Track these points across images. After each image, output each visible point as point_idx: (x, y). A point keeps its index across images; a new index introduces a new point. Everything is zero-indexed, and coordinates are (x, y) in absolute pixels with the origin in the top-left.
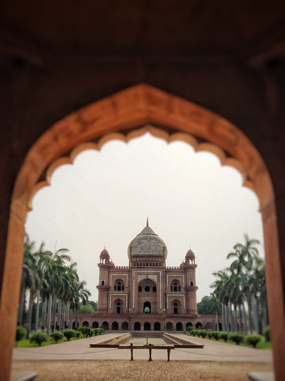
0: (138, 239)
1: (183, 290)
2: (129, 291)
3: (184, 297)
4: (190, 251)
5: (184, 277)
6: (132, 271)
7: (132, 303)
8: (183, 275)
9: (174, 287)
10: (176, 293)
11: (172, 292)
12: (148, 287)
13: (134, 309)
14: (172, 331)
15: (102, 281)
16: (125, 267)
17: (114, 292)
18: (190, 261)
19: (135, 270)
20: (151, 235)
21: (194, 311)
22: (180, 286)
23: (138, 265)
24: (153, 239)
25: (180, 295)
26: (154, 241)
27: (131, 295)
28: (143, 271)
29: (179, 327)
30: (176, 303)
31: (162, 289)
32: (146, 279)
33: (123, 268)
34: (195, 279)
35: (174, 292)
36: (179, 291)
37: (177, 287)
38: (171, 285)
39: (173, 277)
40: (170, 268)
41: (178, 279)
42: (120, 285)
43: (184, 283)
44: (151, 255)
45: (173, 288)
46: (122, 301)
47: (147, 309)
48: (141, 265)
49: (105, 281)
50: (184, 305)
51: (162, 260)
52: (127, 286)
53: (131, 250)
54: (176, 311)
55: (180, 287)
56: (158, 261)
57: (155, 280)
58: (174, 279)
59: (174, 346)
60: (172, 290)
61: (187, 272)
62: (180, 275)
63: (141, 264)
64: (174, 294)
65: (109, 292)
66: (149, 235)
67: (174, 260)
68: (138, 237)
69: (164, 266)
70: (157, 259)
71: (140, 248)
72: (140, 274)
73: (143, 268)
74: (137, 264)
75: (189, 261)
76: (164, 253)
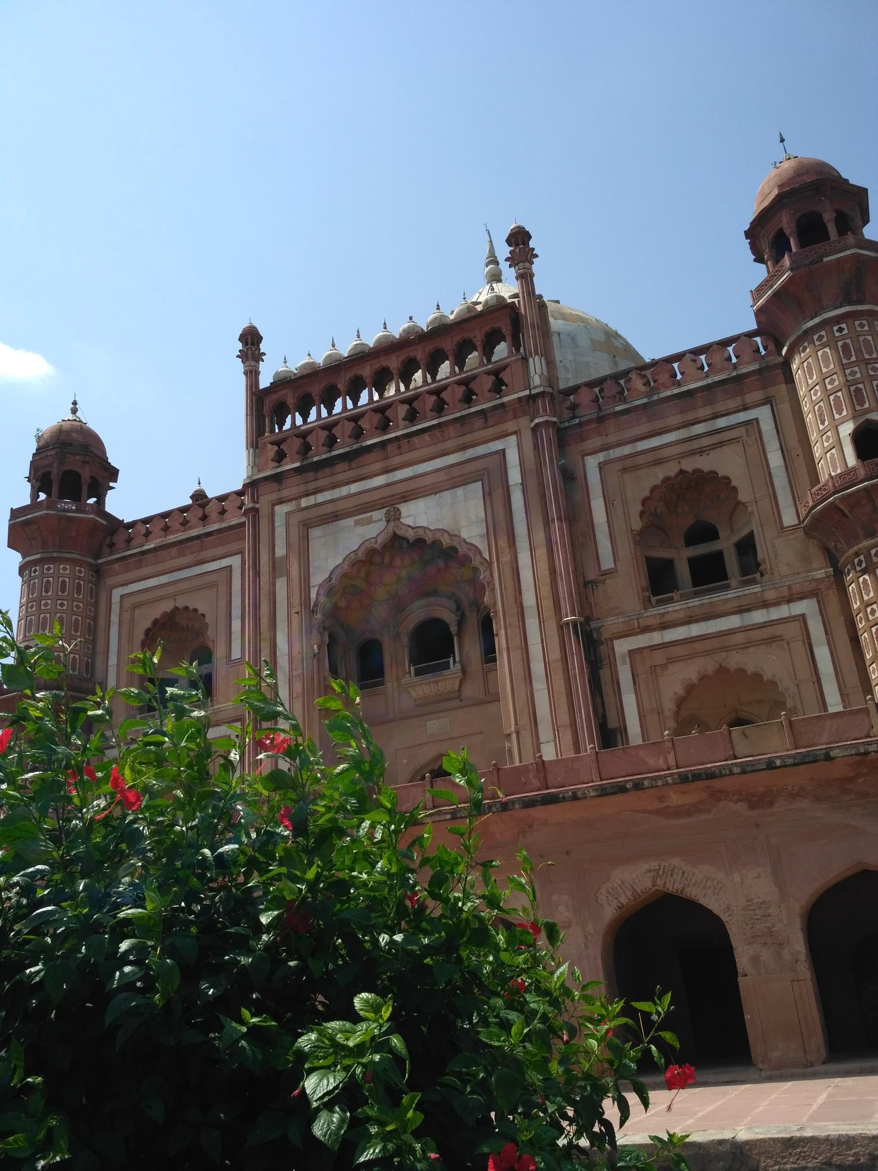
5: (767, 426)
8: (763, 414)
9: (692, 561)
10: (716, 597)
25: (758, 616)
28: (354, 488)
31: (546, 590)
32: (380, 540)
39: (659, 462)
41: (705, 463)
57: (465, 535)
58: (659, 474)
62: (722, 423)
64: (690, 620)
69: (536, 381)
72: (332, 516)
76: (526, 278)
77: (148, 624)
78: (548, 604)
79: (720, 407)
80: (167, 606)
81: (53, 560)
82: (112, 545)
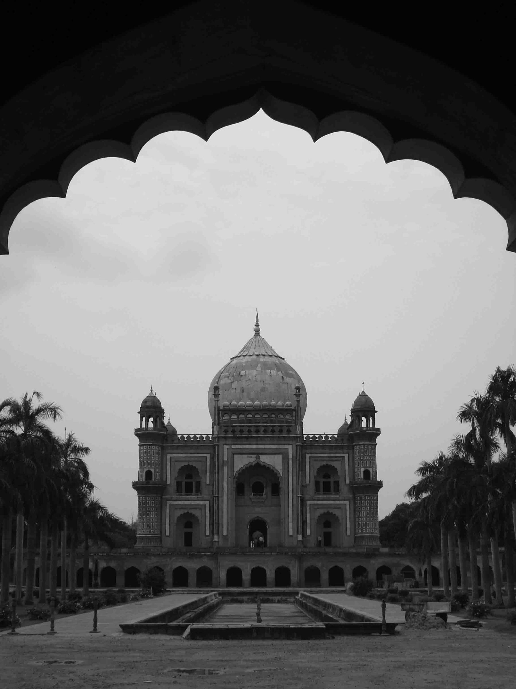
0: (236, 367)
1: (344, 489)
2: (213, 492)
3: (348, 507)
4: (363, 395)
5: (347, 459)
6: (218, 445)
7: (220, 522)
8: (346, 455)
9: (324, 482)
11: (320, 495)
12: (258, 482)
13: (225, 538)
14: (319, 586)
15: (145, 470)
16: (201, 437)
17: (175, 497)
18: (364, 419)
19: (228, 442)
20: (267, 359)
21: (372, 538)
22: (338, 482)
23: (234, 432)
24: (271, 369)
25: (337, 502)
26: (274, 372)
27: (218, 503)
28: (247, 446)
29: (336, 579)
30: (328, 521)
32: (254, 464)
33: (198, 440)
34: (375, 464)
35: (324, 494)
36: (335, 491)
37: (329, 482)
38: (315, 477)
39: (323, 461)
40: (314, 437)
41: (333, 464)
42: (189, 480)
43: (347, 473)
44: (266, 406)
45: (321, 484)
46: (197, 517)
47: (257, 533)
48: (241, 431)
49: (153, 470)
50: (348, 526)
51: (294, 418)
52: (208, 482)
53: (216, 395)
54: (328, 539)
55: (337, 483)
56: (283, 422)
59: (324, 627)
60: (317, 490)
61: (356, 448)
62: (338, 455)
63: (242, 428)
65: (164, 497)
66: (261, 359)
67: (323, 418)
68: (234, 362)
69: (298, 432)
70: (282, 417)
71: (239, 390)
72: (241, 453)
73: (247, 438)
74: (231, 429)
75: (360, 421)
76: (298, 401)
77: (180, 468)
78: (295, 491)
79: (339, 451)
80: (186, 464)
81: (155, 445)
82: (167, 440)
